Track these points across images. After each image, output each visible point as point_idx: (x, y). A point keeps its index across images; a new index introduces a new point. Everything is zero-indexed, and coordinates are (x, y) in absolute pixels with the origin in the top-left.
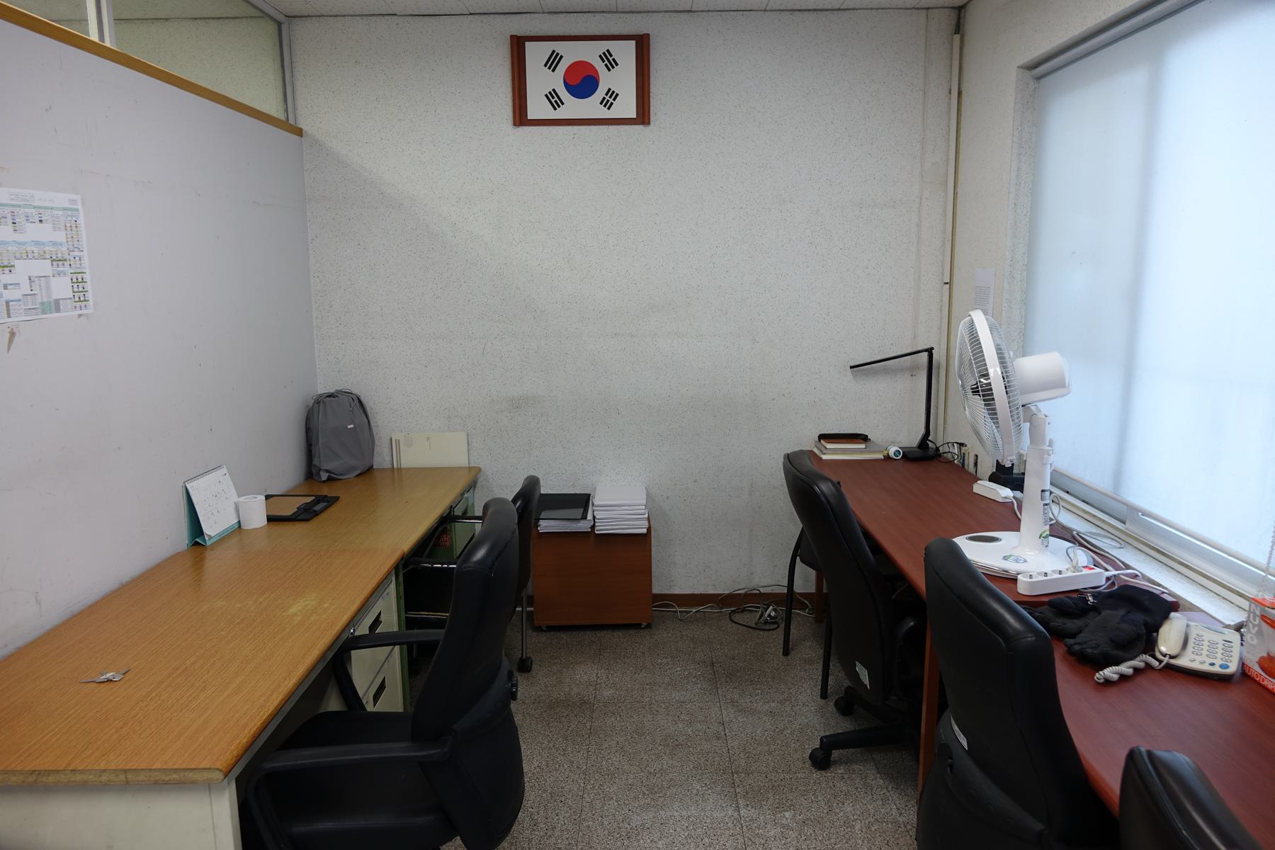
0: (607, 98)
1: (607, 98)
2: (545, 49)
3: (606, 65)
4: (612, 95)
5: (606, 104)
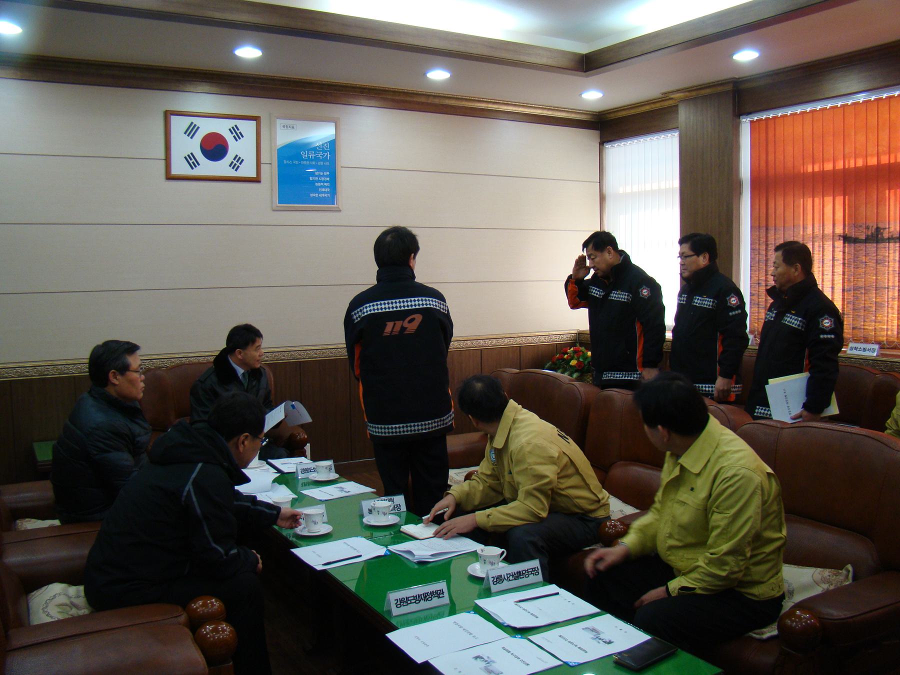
2: (185, 122)
3: (234, 137)
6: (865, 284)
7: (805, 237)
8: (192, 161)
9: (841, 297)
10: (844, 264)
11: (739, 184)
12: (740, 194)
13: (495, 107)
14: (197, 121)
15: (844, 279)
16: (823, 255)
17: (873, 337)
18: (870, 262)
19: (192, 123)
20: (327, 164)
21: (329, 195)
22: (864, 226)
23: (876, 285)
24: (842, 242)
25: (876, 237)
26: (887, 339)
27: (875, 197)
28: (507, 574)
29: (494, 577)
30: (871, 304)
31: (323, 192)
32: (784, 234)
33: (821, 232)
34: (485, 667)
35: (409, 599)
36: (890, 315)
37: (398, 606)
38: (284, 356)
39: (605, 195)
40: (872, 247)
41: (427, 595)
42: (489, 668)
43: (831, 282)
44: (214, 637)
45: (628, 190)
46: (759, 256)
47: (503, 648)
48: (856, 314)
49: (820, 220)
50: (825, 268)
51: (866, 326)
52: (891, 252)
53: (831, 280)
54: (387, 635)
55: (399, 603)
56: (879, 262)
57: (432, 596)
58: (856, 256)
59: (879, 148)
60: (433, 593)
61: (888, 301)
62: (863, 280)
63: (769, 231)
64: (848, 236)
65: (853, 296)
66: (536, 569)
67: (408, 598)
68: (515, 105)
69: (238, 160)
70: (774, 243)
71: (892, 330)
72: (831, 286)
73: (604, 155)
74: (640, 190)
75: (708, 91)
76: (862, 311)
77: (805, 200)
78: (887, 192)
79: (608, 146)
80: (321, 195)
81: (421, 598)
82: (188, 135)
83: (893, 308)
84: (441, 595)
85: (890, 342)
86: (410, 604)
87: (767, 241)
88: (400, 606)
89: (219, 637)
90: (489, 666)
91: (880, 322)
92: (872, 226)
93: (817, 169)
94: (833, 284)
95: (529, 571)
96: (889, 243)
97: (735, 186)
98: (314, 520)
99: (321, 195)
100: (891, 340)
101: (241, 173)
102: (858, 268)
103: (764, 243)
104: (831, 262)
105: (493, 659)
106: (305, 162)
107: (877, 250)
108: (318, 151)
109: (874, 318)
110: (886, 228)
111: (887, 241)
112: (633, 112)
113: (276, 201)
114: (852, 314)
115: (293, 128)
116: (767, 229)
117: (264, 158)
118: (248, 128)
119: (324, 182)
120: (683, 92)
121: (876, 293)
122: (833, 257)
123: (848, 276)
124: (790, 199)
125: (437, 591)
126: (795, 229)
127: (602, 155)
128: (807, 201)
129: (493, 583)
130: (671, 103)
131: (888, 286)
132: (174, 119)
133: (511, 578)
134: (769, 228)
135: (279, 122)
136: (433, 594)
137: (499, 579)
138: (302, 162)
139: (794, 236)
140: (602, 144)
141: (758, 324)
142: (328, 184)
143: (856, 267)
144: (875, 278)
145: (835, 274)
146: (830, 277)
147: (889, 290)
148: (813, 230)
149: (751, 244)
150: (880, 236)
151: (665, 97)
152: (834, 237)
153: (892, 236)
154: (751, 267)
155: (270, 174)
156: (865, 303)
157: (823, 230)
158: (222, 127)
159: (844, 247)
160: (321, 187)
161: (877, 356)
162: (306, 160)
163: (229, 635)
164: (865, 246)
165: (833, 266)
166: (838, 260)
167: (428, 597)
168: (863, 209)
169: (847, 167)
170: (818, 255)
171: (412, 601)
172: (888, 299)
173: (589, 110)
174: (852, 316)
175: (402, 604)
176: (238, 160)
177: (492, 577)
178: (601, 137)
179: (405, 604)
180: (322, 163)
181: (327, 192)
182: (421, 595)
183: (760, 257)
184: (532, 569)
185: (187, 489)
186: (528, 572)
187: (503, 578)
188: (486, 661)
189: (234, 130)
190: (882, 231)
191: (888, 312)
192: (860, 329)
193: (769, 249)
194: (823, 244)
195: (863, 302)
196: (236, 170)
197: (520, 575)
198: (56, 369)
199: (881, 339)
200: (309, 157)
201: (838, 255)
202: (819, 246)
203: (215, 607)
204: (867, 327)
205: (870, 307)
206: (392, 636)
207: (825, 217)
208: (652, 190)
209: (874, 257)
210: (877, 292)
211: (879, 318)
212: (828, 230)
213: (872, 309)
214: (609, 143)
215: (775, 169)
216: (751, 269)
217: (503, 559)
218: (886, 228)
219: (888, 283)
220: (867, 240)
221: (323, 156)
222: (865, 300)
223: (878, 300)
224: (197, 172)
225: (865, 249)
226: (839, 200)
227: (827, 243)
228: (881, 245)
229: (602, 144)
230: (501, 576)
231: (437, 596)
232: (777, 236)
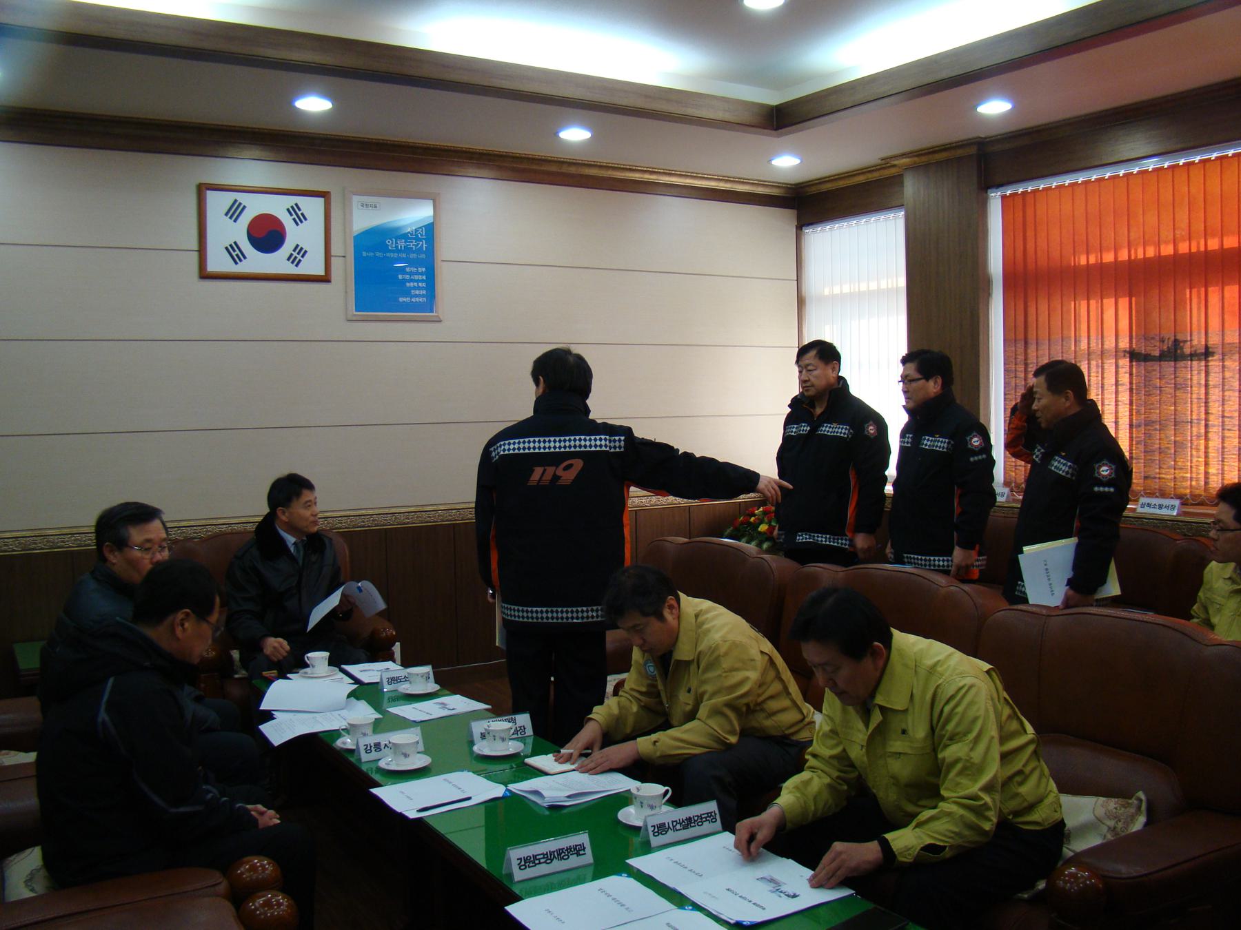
0: (295, 254)
1: (295, 254)
2: (228, 198)
3: (294, 219)
4: (299, 254)
6: (1160, 417)
7: (1078, 353)
9: (1128, 435)
10: (1131, 390)
11: (988, 282)
12: (988, 295)
13: (653, 178)
14: (243, 198)
15: (1131, 411)
16: (1103, 378)
17: (1172, 489)
18: (1166, 387)
19: (236, 201)
20: (423, 256)
21: (425, 299)
22: (1157, 338)
23: (1175, 418)
24: (1128, 360)
25: (1174, 353)
26: (1191, 492)
27: (1172, 298)
28: (673, 822)
29: (654, 826)
30: (1168, 444)
31: (416, 296)
32: (1049, 349)
33: (1100, 346)
35: (538, 857)
36: (1195, 460)
37: (523, 867)
39: (805, 298)
40: (1168, 367)
41: (563, 852)
43: (1114, 414)
45: (837, 290)
46: (1016, 380)
48: (1150, 458)
49: (1097, 329)
50: (1106, 396)
51: (1163, 474)
52: (1195, 372)
53: (1114, 412)
54: (506, 908)
55: (523, 863)
56: (1179, 386)
57: (568, 853)
58: (1147, 379)
59: (1176, 232)
61: (1191, 440)
62: (1158, 411)
63: (1029, 345)
64: (1136, 351)
65: (1145, 433)
66: (713, 814)
67: (536, 856)
68: (681, 176)
69: (300, 252)
70: (1035, 361)
71: (1198, 479)
72: (1114, 420)
74: (852, 291)
75: (944, 155)
76: (1157, 453)
77: (1077, 302)
78: (1188, 291)
80: (413, 300)
81: (554, 856)
82: (231, 218)
83: (1198, 450)
84: (582, 852)
85: (1195, 496)
87: (1026, 359)
89: (272, 914)
91: (1181, 469)
92: (1169, 339)
93: (1092, 260)
94: (1117, 418)
95: (703, 816)
96: (1191, 360)
97: (984, 284)
98: (404, 751)
99: (413, 300)
100: (1197, 493)
101: (302, 270)
102: (1150, 395)
103: (1022, 363)
104: (1114, 387)
106: (392, 255)
107: (1175, 371)
108: (409, 238)
109: (1173, 463)
110: (1187, 341)
111: (1189, 358)
112: (841, 184)
114: (1143, 457)
115: (376, 207)
116: (1026, 343)
117: (336, 249)
118: (313, 208)
119: (418, 281)
120: (909, 157)
121: (1175, 429)
122: (1117, 381)
123: (1136, 406)
124: (1056, 303)
125: (576, 846)
126: (1064, 343)
128: (1080, 305)
129: (654, 835)
130: (893, 171)
131: (1191, 419)
132: (211, 196)
133: (678, 827)
134: (1030, 341)
135: (356, 199)
136: (571, 851)
137: (661, 829)
138: (388, 255)
139: (1062, 352)
140: (800, 227)
141: (1015, 472)
142: (424, 285)
143: (1148, 394)
144: (1173, 408)
145: (1120, 403)
146: (1112, 408)
147: (1193, 424)
148: (1089, 344)
149: (1004, 364)
150: (1179, 351)
151: (886, 163)
152: (1117, 353)
153: (1195, 351)
154: (1005, 394)
155: (343, 270)
156: (1160, 444)
157: (1102, 345)
158: (277, 207)
159: (1131, 367)
160: (414, 288)
161: (1178, 515)
164: (1160, 365)
165: (1117, 392)
166: (1122, 385)
167: (563, 854)
168: (1155, 315)
169: (1133, 258)
170: (1095, 378)
171: (542, 861)
172: (1191, 437)
173: (782, 181)
174: (1142, 461)
176: (299, 254)
177: (652, 826)
178: (799, 218)
179: (531, 865)
180: (415, 255)
181: (423, 296)
183: (1017, 381)
184: (707, 814)
185: (100, 720)
186: (702, 819)
187: (667, 827)
189: (294, 211)
190: (1182, 344)
191: (1191, 455)
192: (1155, 478)
193: (1029, 370)
194: (1102, 363)
195: (1158, 442)
196: (297, 265)
197: (691, 823)
198: (47, 541)
199: (1182, 491)
200: (397, 247)
201: (1123, 377)
202: (1097, 366)
203: (267, 872)
204: (1163, 476)
205: (1168, 448)
206: (513, 909)
207: (1105, 326)
209: (1171, 379)
210: (1177, 427)
211: (1180, 464)
212: (1110, 343)
213: (1169, 452)
214: (810, 227)
215: (1036, 262)
216: (1005, 398)
217: (668, 801)
218: (1187, 341)
219: (1191, 415)
220: (1162, 357)
221: (416, 246)
222: (1160, 439)
223: (1178, 439)
224: (243, 268)
225: (1160, 369)
226: (1124, 302)
227: (1109, 361)
228: (1181, 364)
229: (800, 227)
230: (664, 824)
232: (1040, 352)
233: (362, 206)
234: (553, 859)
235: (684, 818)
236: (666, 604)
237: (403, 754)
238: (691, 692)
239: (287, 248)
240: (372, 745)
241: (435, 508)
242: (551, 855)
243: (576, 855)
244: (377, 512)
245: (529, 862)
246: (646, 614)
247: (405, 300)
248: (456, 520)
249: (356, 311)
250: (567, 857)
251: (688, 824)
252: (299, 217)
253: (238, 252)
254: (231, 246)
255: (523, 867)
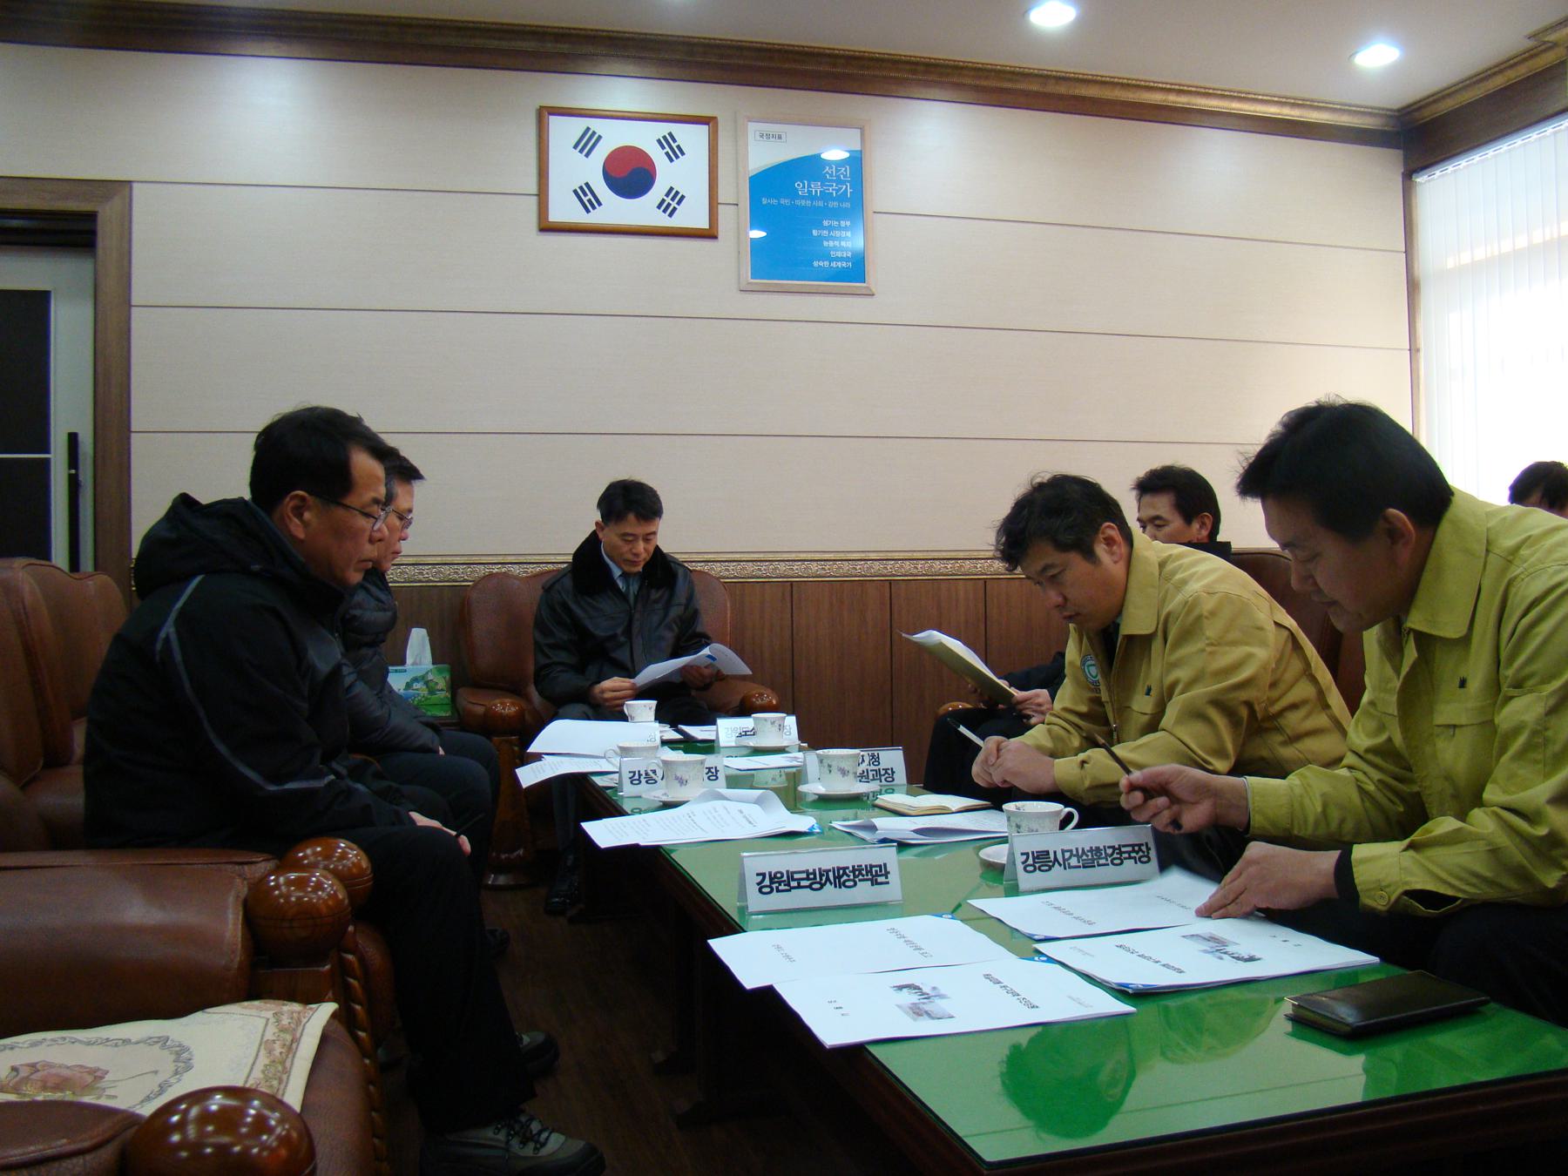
0: (668, 200)
1: (668, 200)
2: (579, 125)
3: (667, 154)
5: (666, 207)
8: (587, 198)
13: (1182, 100)
14: (596, 125)
19: (588, 129)
28: (1063, 851)
29: (1027, 854)
34: (915, 1004)
37: (765, 890)
38: (760, 570)
42: (921, 1006)
44: (287, 896)
45: (1466, 258)
47: (987, 976)
54: (709, 941)
55: (767, 882)
57: (855, 876)
60: (860, 871)
66: (1144, 848)
67: (793, 873)
68: (1223, 97)
69: (674, 198)
73: (1414, 201)
79: (1421, 179)
80: (834, 264)
81: (828, 879)
82: (581, 151)
84: (881, 879)
86: (794, 888)
88: (768, 890)
89: (299, 898)
90: (924, 1003)
95: (1123, 849)
98: (679, 775)
99: (834, 264)
101: (677, 221)
105: (943, 992)
106: (803, 202)
113: (747, 273)
115: (780, 137)
117: (724, 195)
118: (693, 138)
125: (871, 866)
127: (1410, 200)
129: (1025, 869)
132: (555, 122)
133: (1074, 861)
135: (753, 128)
136: (860, 874)
137: (1041, 860)
138: (798, 202)
140: (1409, 175)
158: (645, 138)
162: (803, 198)
163: (325, 901)
167: (845, 878)
171: (803, 883)
173: (1381, 105)
175: (774, 886)
176: (674, 198)
177: (1022, 854)
178: (1406, 163)
180: (836, 203)
182: (827, 871)
184: (1133, 846)
186: (1121, 853)
187: (1052, 859)
188: (923, 994)
189: (667, 142)
196: (670, 215)
203: (345, 862)
206: (719, 945)
208: (1514, 250)
221: (837, 191)
224: (596, 217)
229: (1409, 175)
230: (1048, 852)
231: (871, 880)
233: (762, 136)
234: (826, 882)
235: (1087, 848)
236: (1101, 536)
237: (677, 778)
238: (1152, 693)
239: (657, 192)
240: (643, 772)
241: (862, 556)
242: (821, 876)
243: (869, 882)
244: (779, 556)
245: (780, 883)
246: (1063, 547)
247: (821, 264)
248: (894, 575)
249: (752, 278)
250: (851, 883)
251: (1093, 860)
252: (674, 151)
253: (590, 196)
254: (581, 188)
255: (765, 890)
